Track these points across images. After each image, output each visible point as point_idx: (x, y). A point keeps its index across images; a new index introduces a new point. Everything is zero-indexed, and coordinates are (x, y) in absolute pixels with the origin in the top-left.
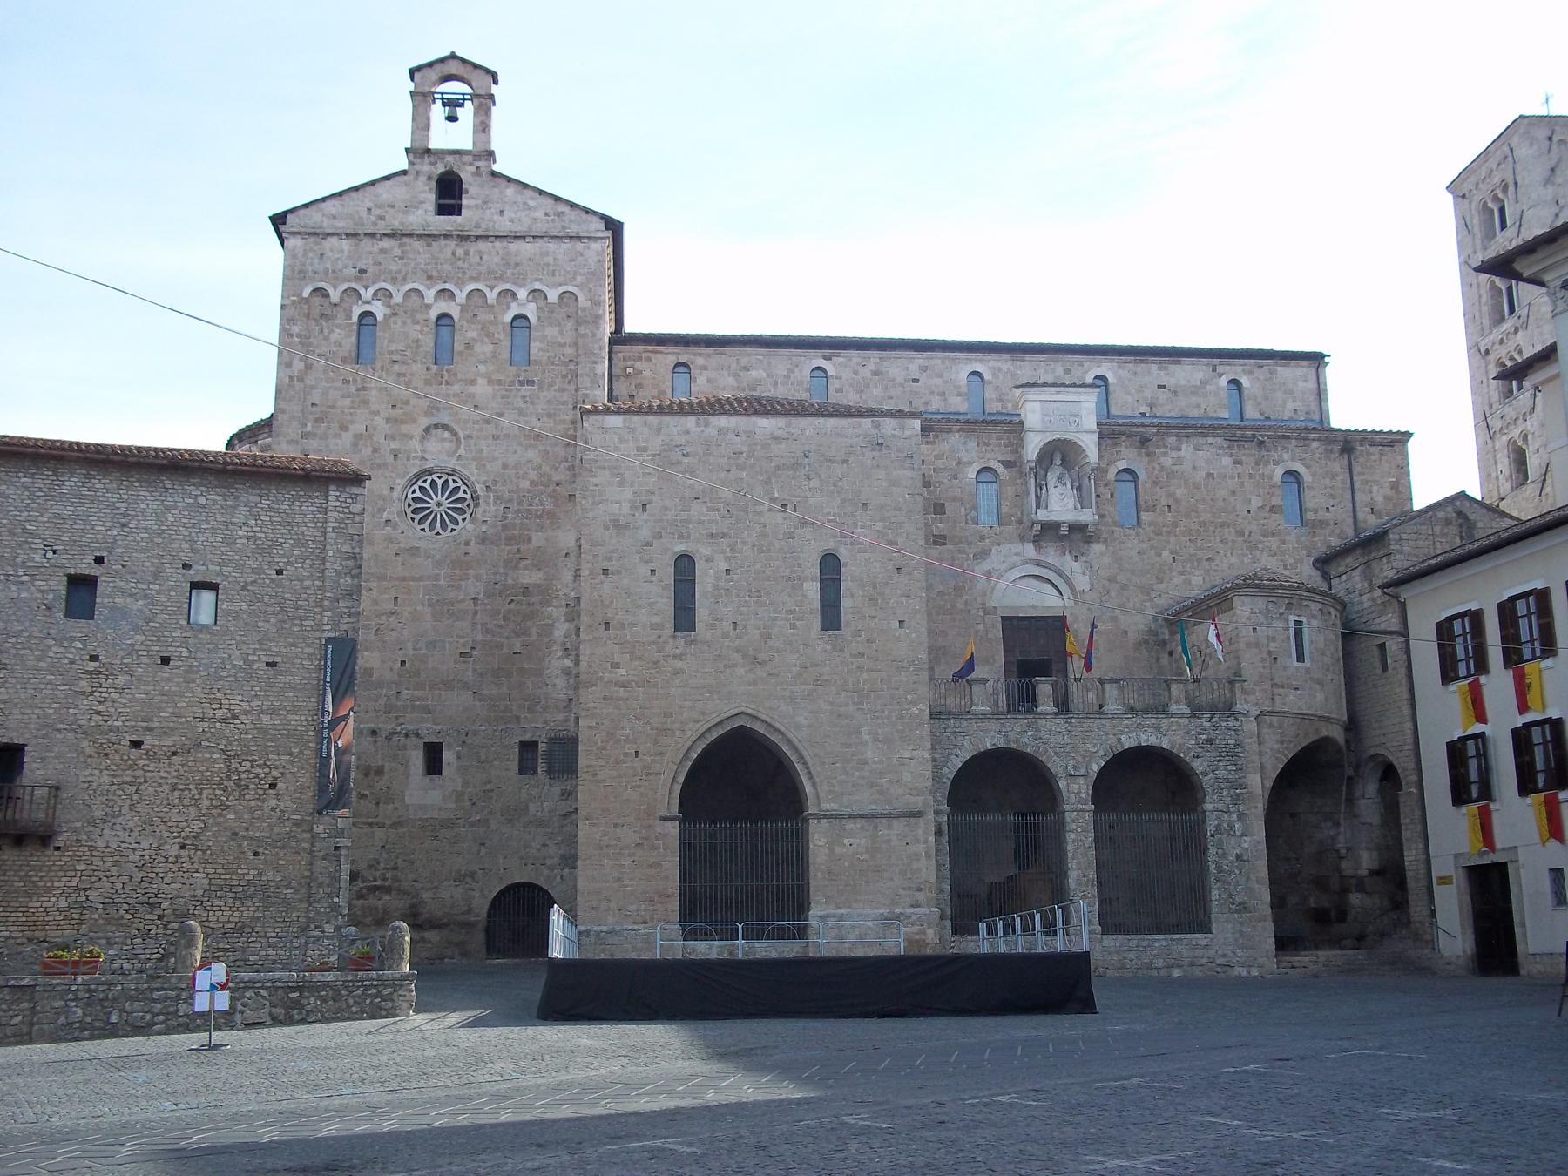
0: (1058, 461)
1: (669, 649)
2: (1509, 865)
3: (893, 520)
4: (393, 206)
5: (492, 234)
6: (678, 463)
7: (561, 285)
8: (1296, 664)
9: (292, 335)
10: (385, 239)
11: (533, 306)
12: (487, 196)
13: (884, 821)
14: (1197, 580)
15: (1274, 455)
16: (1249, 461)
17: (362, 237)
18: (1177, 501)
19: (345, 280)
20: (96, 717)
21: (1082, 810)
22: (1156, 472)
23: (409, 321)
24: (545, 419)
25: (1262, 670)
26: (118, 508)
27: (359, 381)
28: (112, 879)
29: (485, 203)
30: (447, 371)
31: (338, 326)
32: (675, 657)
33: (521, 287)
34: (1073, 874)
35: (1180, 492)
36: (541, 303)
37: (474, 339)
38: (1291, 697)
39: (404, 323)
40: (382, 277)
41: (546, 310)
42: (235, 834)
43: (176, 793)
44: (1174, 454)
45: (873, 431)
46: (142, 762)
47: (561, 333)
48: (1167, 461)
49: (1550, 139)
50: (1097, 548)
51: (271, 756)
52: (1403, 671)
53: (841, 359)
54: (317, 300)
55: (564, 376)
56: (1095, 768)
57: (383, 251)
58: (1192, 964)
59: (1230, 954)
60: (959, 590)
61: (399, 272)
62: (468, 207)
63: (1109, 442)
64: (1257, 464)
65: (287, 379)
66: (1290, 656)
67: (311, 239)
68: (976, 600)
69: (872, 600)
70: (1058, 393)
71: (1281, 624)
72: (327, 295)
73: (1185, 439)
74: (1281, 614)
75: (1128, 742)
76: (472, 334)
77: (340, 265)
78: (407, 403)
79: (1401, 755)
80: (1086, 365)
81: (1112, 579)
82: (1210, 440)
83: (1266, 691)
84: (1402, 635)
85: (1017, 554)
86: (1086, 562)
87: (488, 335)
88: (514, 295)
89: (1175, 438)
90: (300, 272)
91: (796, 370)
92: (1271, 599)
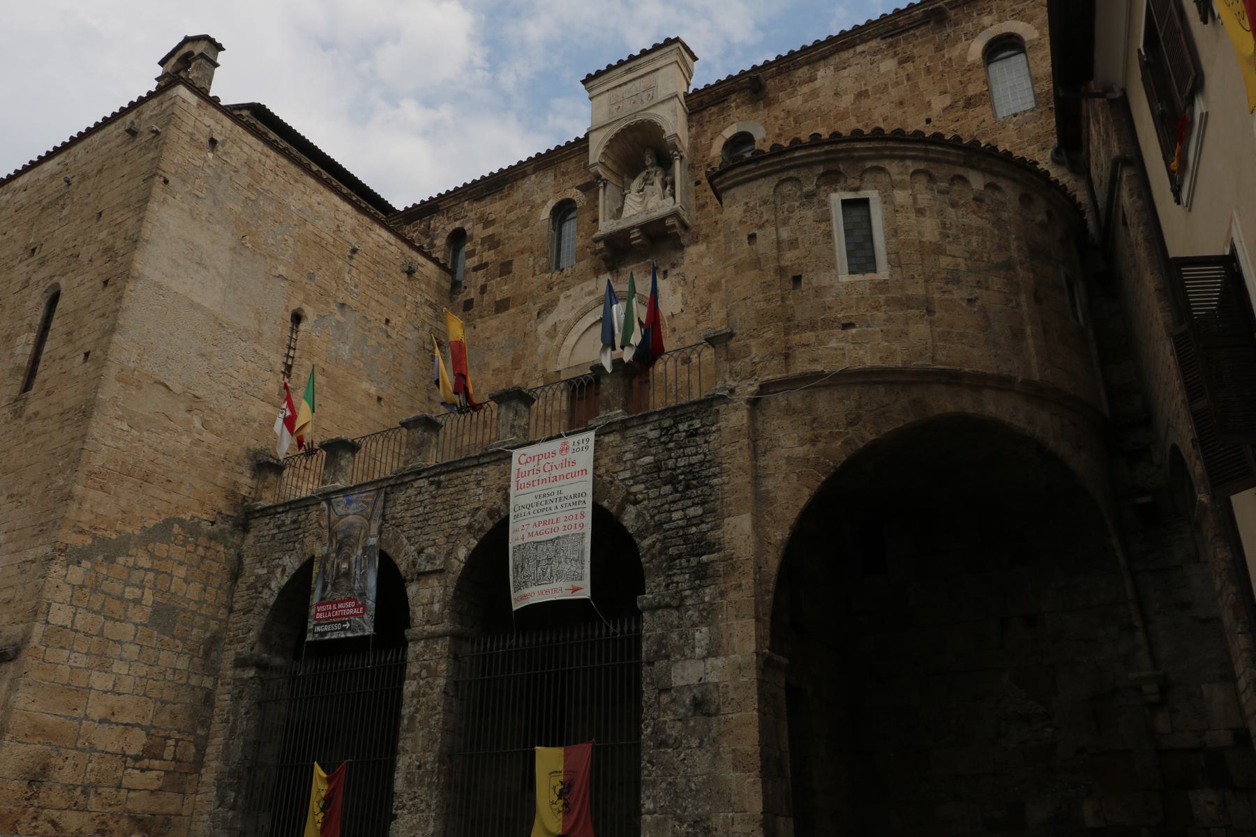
0: (649, 161)
8: (845, 277)
15: (969, 27)
22: (781, 122)
25: (762, 305)
34: (402, 762)
38: (833, 344)
48: (795, 102)
50: (693, 251)
56: (462, 553)
60: (516, 362)
63: (714, 109)
66: (832, 266)
68: (535, 368)
70: (629, 71)
71: (809, 214)
73: (822, 62)
74: (810, 196)
81: (713, 287)
82: (859, 49)
83: (771, 343)
85: (591, 293)
86: (678, 274)
89: (805, 69)
92: (784, 176)
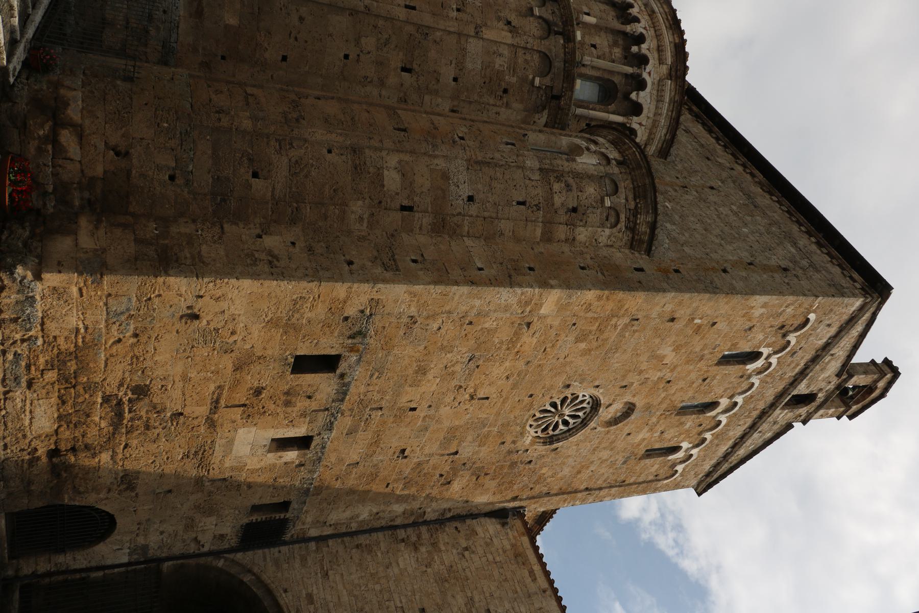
9: (786, 307)
17: (819, 353)
24: (591, 474)
72: (797, 329)
78: (666, 391)
88: (697, 446)
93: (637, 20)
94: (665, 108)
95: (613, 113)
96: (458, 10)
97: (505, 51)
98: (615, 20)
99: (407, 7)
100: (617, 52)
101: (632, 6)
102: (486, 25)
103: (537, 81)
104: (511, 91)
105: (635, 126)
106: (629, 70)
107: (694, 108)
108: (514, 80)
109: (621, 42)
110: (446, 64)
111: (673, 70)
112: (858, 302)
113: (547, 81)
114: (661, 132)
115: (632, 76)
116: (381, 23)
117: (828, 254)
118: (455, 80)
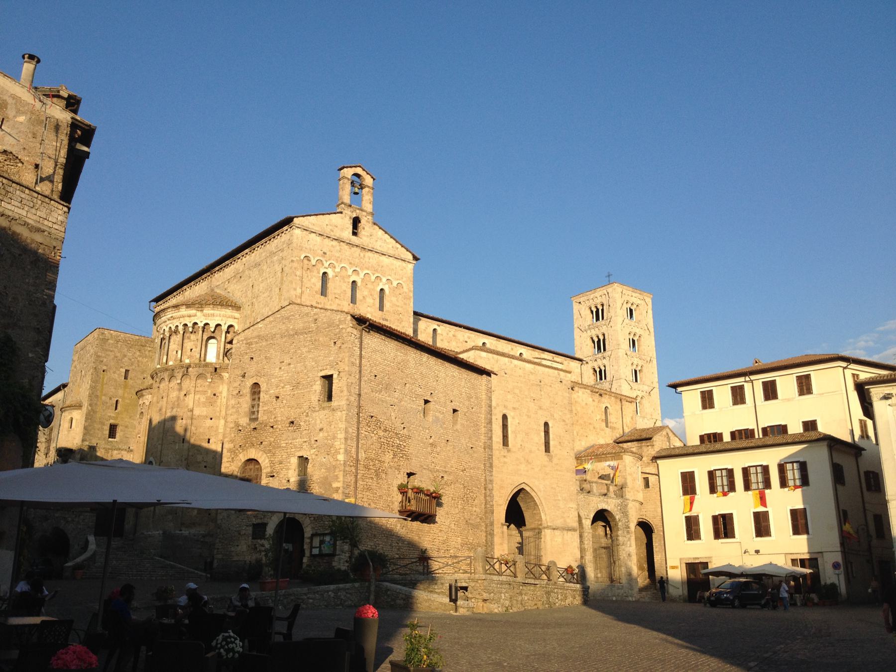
1: (502, 453)
2: (709, 564)
3: (564, 412)
4: (337, 227)
5: (374, 250)
6: (503, 376)
7: (397, 280)
9: (296, 276)
10: (334, 240)
11: (387, 286)
12: (372, 233)
13: (566, 532)
14: (583, 443)
16: (596, 400)
18: (578, 412)
19: (317, 255)
20: (433, 464)
21: (589, 533)
23: (342, 281)
26: (435, 373)
27: (322, 304)
28: (439, 538)
29: (371, 236)
30: (356, 307)
31: (314, 276)
32: (504, 456)
33: (384, 276)
35: (579, 409)
36: (391, 286)
37: (366, 295)
39: (340, 281)
40: (333, 258)
41: (393, 290)
42: (467, 521)
43: (453, 501)
44: (577, 394)
45: (558, 376)
46: (445, 487)
47: (397, 300)
49: (622, 293)
51: (474, 488)
52: (658, 489)
53: (443, 327)
54: (306, 261)
55: (398, 320)
57: (332, 246)
58: (618, 595)
59: (627, 592)
61: (339, 257)
62: (365, 235)
64: (599, 402)
65: (294, 296)
67: (305, 232)
69: (560, 443)
75: (600, 508)
76: (366, 293)
77: (316, 248)
79: (654, 520)
80: (518, 348)
84: (656, 475)
87: (371, 295)
88: (381, 279)
90: (300, 246)
91: (428, 328)
93: (177, 326)
94: (216, 312)
95: (221, 337)
96: (182, 419)
97: (197, 397)
98: (178, 336)
99: (183, 442)
100: (193, 337)
101: (170, 327)
102: (187, 406)
103: (209, 380)
104: (214, 392)
105: (226, 327)
106: (201, 332)
107: (217, 268)
108: (209, 391)
109: (188, 335)
110: (205, 424)
111: (198, 309)
112: (297, 232)
113: (208, 375)
114: (229, 312)
115: (203, 331)
116: (190, 454)
117: (278, 235)
118: (211, 419)
